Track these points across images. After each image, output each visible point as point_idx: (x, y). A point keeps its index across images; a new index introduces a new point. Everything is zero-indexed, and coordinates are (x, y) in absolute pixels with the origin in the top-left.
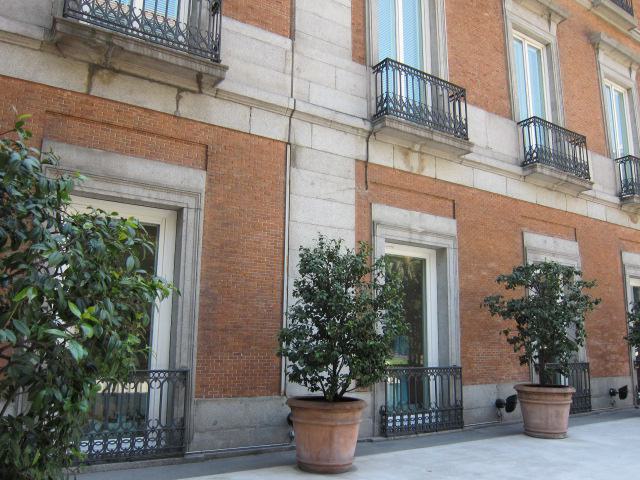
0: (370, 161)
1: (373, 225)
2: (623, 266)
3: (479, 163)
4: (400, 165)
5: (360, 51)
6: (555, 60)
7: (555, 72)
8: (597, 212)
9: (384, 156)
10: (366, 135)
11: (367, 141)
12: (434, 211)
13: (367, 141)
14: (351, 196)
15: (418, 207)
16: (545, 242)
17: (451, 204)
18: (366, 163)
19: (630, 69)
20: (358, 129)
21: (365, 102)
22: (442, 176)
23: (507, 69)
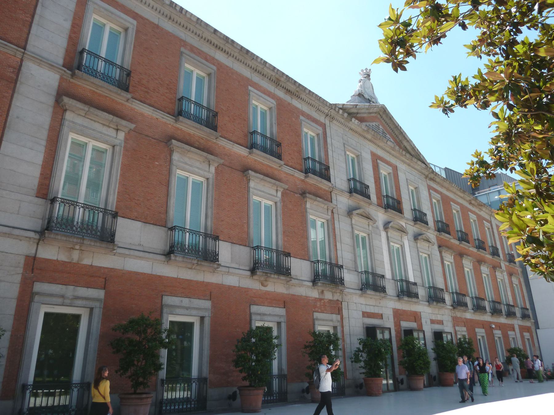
0: (37, 256)
1: (32, 295)
2: (250, 314)
3: (129, 255)
4: (63, 257)
5: (45, 191)
6: (211, 187)
7: (210, 195)
8: (231, 281)
9: (50, 252)
10: (37, 241)
11: (38, 244)
12: (88, 286)
13: (38, 244)
14: (18, 278)
15: (76, 284)
16: (182, 301)
17: (104, 280)
18: (35, 258)
19: (277, 190)
20: (30, 238)
21: (40, 221)
22: (95, 264)
23: (168, 196)
